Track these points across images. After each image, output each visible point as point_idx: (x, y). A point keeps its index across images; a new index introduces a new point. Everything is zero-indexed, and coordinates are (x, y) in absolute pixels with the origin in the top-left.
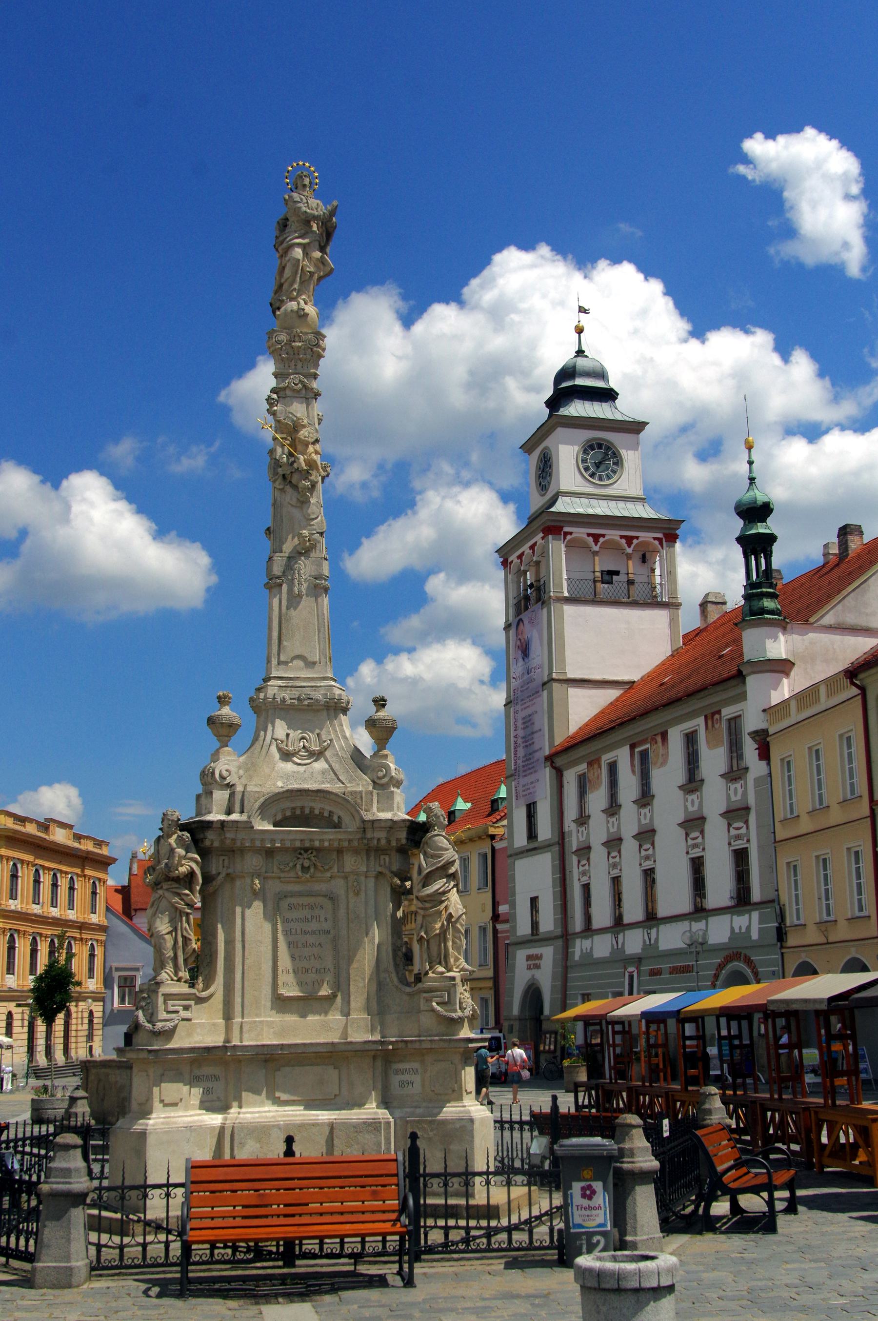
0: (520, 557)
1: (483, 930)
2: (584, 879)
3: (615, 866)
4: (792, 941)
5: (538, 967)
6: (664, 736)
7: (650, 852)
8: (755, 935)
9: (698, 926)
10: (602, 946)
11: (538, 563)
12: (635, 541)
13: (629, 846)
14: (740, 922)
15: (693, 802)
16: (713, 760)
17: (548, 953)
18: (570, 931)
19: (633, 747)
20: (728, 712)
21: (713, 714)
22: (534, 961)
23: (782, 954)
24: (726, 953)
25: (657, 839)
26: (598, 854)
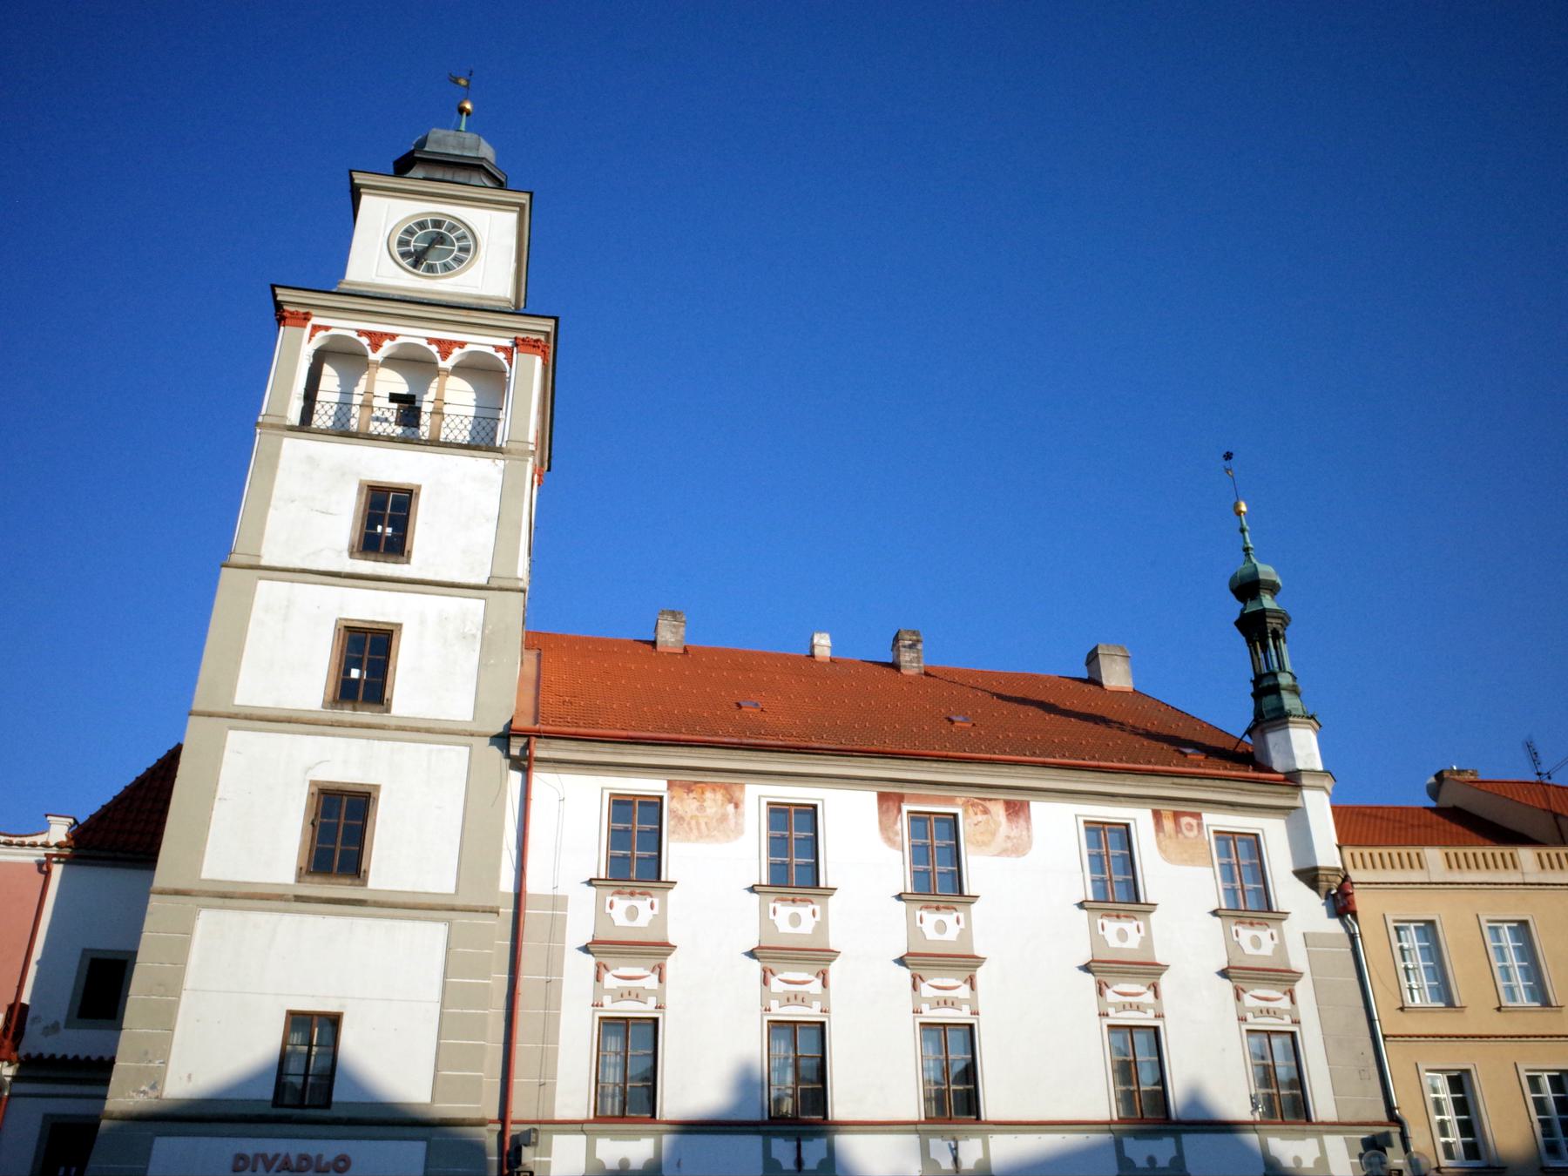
6: (1016, 810)
19: (889, 800)
20: (1215, 820)
21: (1177, 816)
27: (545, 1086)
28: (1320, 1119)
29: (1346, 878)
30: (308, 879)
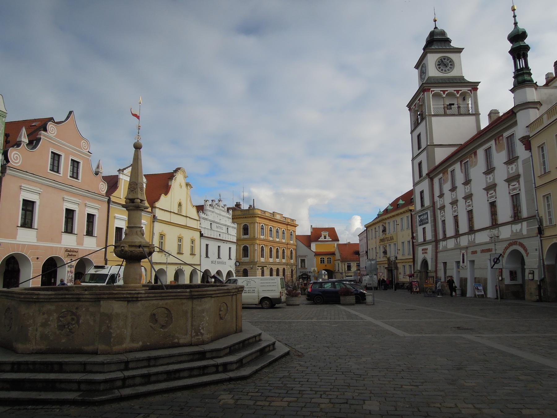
0: (415, 105)
1: (409, 242)
2: (443, 219)
3: (455, 211)
4: (547, 233)
5: (426, 253)
6: (475, 153)
7: (470, 203)
8: (525, 232)
9: (495, 232)
10: (451, 244)
11: (422, 105)
12: (460, 92)
13: (461, 203)
15: (490, 178)
16: (499, 158)
17: (430, 247)
18: (438, 239)
19: (461, 162)
20: (506, 134)
21: (499, 138)
22: (425, 251)
23: (541, 240)
24: (508, 242)
25: (473, 198)
26: (448, 208)
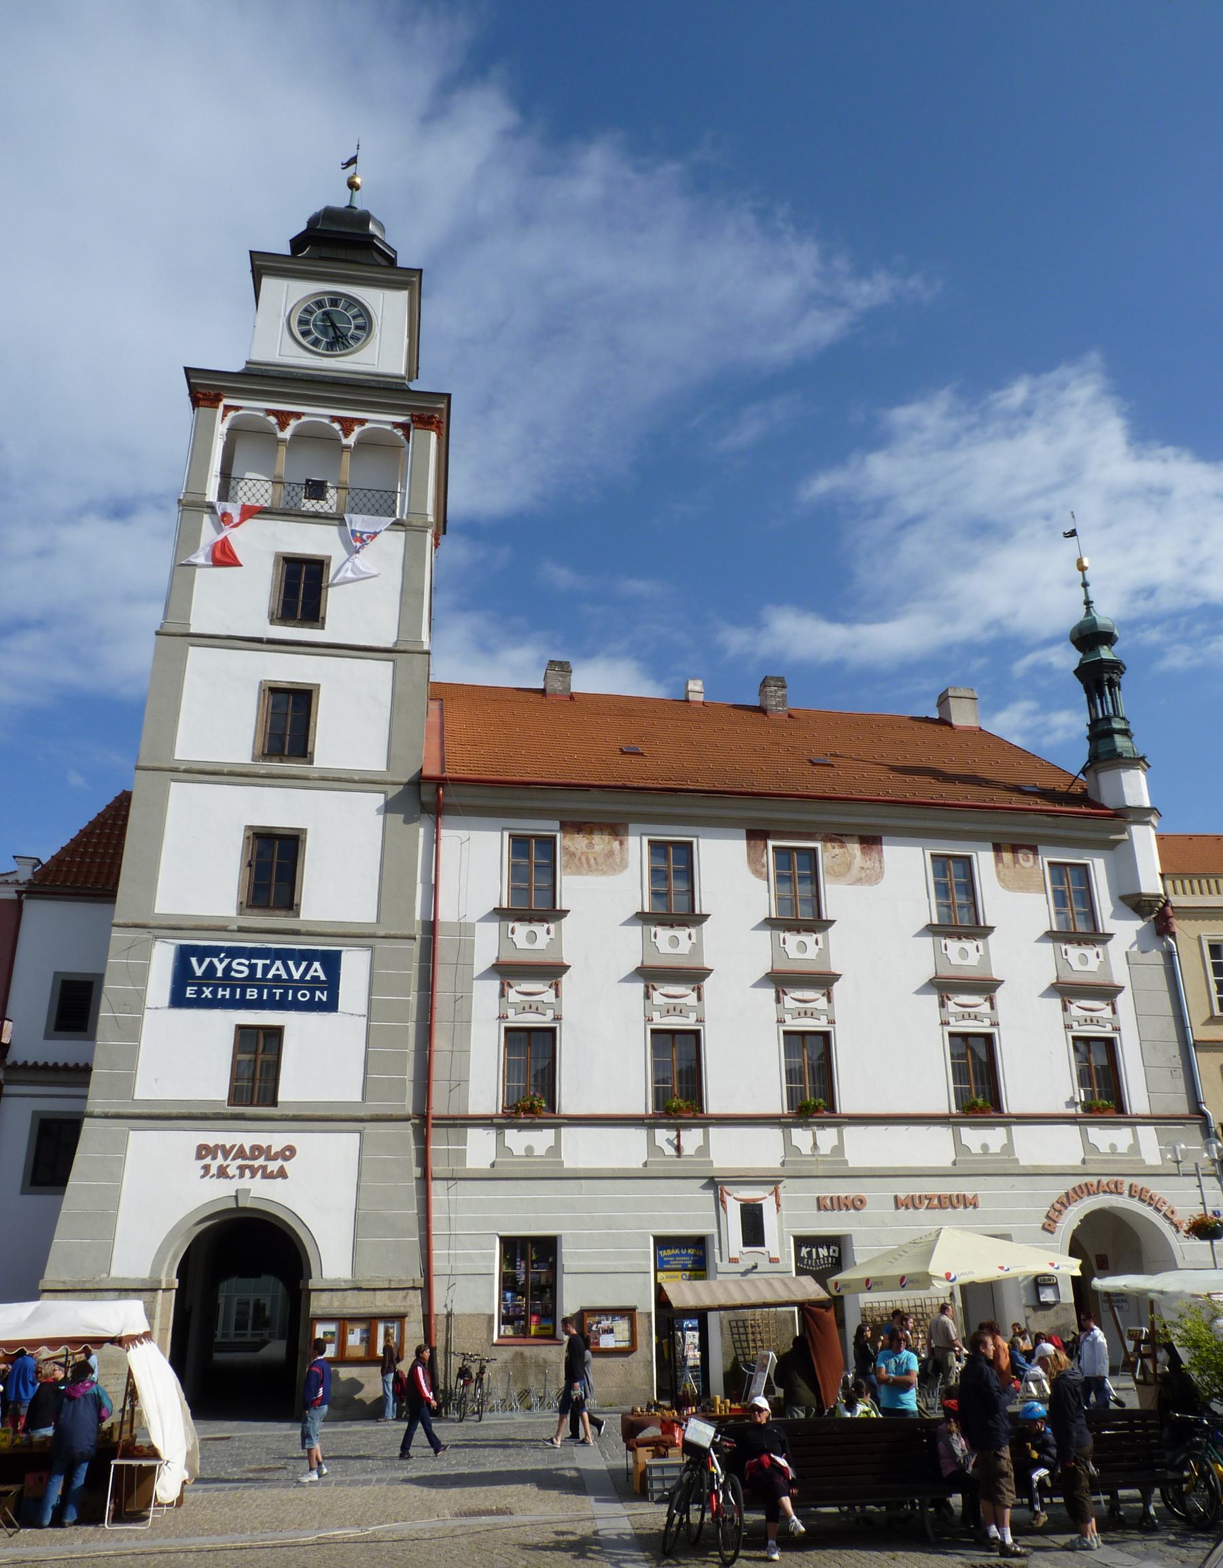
14: (1106, 1138)
18: (438, 1107)
27: (460, 1083)
28: (1134, 1112)
29: (1167, 903)
30: (249, 911)
